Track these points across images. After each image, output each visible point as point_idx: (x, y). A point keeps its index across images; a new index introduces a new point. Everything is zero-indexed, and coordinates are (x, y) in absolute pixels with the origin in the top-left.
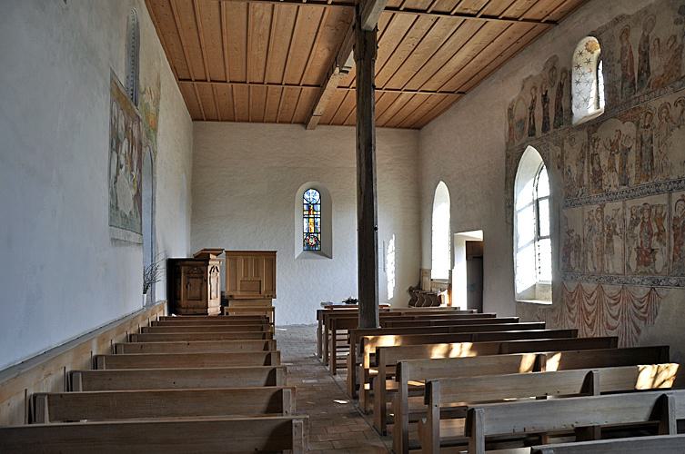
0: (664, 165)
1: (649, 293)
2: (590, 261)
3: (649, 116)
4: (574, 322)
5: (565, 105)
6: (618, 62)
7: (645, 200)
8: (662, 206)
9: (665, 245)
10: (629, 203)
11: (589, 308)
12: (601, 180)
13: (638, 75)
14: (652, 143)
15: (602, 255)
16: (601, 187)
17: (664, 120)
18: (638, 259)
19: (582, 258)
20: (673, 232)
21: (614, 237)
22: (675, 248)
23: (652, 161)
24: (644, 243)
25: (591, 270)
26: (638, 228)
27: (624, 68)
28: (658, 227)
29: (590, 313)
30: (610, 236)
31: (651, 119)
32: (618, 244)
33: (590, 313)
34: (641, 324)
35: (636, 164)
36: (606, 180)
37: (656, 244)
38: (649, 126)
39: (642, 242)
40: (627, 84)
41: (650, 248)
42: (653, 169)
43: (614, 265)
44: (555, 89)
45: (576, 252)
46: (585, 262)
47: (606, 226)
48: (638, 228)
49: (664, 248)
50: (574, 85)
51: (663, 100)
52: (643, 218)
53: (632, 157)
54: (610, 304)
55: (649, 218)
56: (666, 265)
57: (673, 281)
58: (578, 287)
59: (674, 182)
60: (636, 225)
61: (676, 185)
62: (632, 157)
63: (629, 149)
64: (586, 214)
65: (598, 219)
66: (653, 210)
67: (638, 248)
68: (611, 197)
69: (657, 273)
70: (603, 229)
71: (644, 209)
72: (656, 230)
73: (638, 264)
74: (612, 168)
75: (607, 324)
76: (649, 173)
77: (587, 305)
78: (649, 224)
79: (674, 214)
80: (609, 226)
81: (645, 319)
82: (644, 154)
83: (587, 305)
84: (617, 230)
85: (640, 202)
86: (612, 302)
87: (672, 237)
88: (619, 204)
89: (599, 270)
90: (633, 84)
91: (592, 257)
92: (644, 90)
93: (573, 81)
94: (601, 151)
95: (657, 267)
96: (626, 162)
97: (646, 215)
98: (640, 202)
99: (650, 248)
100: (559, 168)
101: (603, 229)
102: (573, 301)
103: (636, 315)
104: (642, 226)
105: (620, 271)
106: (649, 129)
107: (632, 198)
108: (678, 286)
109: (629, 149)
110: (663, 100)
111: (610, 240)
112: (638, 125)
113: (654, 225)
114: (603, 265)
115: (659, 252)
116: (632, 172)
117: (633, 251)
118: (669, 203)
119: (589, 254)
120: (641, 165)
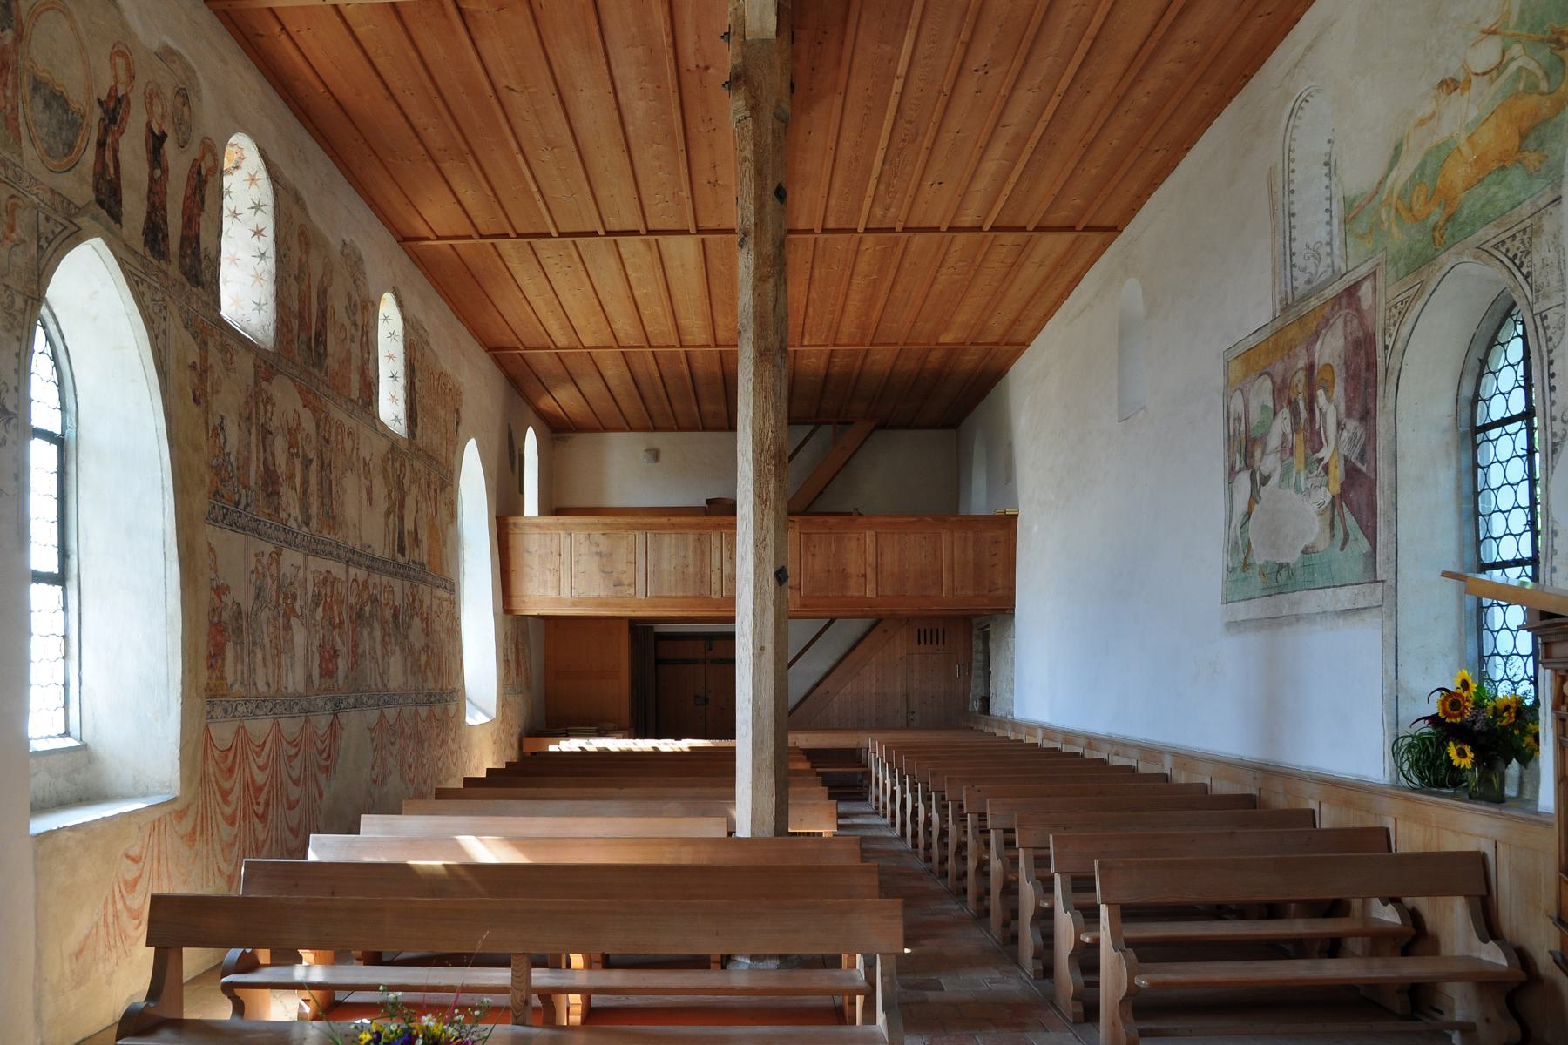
2: (260, 672)
4: (232, 824)
8: (342, 582)
11: (260, 778)
16: (277, 510)
18: (320, 665)
19: (246, 660)
21: (293, 621)
24: (326, 639)
25: (262, 687)
26: (320, 609)
29: (259, 790)
30: (287, 617)
32: (299, 636)
37: (339, 645)
39: (324, 635)
41: (333, 647)
43: (295, 680)
45: (235, 644)
46: (252, 670)
47: (282, 596)
48: (320, 609)
52: (326, 594)
54: (289, 757)
57: (352, 701)
58: (238, 731)
60: (318, 605)
64: (253, 559)
65: (272, 576)
67: (320, 646)
68: (290, 539)
70: (277, 602)
72: (337, 621)
73: (321, 675)
74: (291, 477)
77: (255, 770)
78: (331, 609)
80: (286, 598)
83: (255, 770)
86: (293, 751)
89: (273, 687)
91: (264, 660)
97: (329, 589)
101: (277, 602)
102: (231, 770)
105: (301, 689)
108: (355, 707)
111: (288, 627)
113: (335, 608)
114: (280, 675)
119: (259, 655)
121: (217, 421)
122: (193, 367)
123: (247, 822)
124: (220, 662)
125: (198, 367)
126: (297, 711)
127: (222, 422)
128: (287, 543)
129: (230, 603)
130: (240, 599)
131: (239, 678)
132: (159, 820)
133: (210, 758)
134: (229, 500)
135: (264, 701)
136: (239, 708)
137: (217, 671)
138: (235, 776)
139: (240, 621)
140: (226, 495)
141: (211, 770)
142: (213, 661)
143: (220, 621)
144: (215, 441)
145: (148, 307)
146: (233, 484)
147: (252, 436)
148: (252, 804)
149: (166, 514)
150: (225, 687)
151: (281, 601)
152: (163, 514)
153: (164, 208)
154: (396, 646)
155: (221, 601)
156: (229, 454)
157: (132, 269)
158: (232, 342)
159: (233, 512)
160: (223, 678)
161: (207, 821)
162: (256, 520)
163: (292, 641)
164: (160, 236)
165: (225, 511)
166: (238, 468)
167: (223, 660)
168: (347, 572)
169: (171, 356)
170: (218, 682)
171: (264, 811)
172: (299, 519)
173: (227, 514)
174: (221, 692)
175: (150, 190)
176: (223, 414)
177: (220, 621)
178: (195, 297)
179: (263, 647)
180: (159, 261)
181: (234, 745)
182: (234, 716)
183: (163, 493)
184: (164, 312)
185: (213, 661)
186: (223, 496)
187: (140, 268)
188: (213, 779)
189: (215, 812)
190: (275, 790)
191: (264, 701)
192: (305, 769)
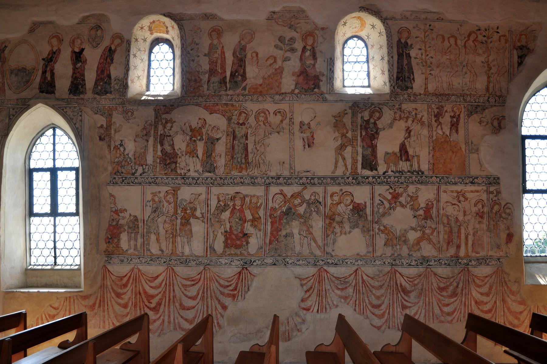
0: (261, 161)
1: (240, 273)
3: (243, 115)
5: (115, 72)
6: (205, 55)
7: (237, 189)
8: (258, 197)
9: (260, 230)
10: (215, 190)
12: (176, 163)
13: (231, 75)
14: (247, 139)
15: (174, 236)
17: (261, 123)
20: (270, 220)
21: (192, 220)
22: (272, 234)
23: (247, 155)
24: (234, 228)
27: (211, 62)
28: (252, 215)
29: (153, 297)
31: (247, 118)
33: (153, 297)
34: (227, 301)
35: (226, 155)
36: (183, 164)
38: (243, 124)
40: (216, 79)
41: (242, 232)
42: (247, 163)
44: (99, 51)
49: (259, 233)
50: (132, 57)
51: (261, 106)
53: (221, 148)
54: (185, 286)
55: (242, 206)
56: (261, 248)
57: (269, 261)
59: (272, 178)
60: (224, 210)
61: (274, 181)
62: (221, 148)
63: (218, 139)
66: (248, 200)
67: (226, 232)
69: (250, 254)
71: (235, 197)
75: (181, 305)
76: (244, 166)
78: (242, 211)
79: (270, 205)
80: (185, 210)
81: (234, 296)
82: (236, 147)
84: (198, 213)
85: (231, 190)
87: (269, 223)
88: (201, 189)
89: (167, 252)
90: (223, 81)
92: (238, 91)
93: (132, 53)
94: (177, 133)
95: (250, 250)
96: (213, 150)
97: (238, 202)
98: (231, 190)
99: (242, 232)
100: (101, 139)
102: (125, 286)
103: (222, 293)
104: (232, 212)
106: (244, 127)
107: (220, 185)
108: (275, 264)
109: (218, 139)
110: (261, 106)
112: (229, 120)
115: (254, 236)
116: (221, 162)
117: (219, 235)
118: (267, 195)
119: (153, 237)
120: (232, 157)
121: (118, 143)
122: (102, 126)
123: (138, 308)
124: (116, 240)
125: (105, 126)
126: (194, 264)
127: (122, 143)
128: (184, 184)
129: (128, 216)
130: (138, 214)
131: (133, 247)
132: (70, 297)
133: (108, 278)
134: (129, 173)
135: (158, 258)
136: (134, 260)
137: (113, 244)
138: (128, 288)
139: (136, 223)
140: (124, 172)
141: (109, 283)
142: (111, 241)
143: (117, 224)
144: (116, 152)
146: (132, 166)
147: (150, 142)
148: (143, 302)
150: (121, 251)
151: (179, 212)
153: (83, 75)
154: (353, 228)
155: (119, 216)
156: (128, 155)
158: (132, 107)
159: (130, 178)
160: (118, 246)
161: (104, 304)
162: (154, 178)
163: (191, 230)
164: (80, 87)
165: (124, 178)
166: (135, 159)
167: (119, 240)
168: (267, 190)
170: (114, 249)
171: (156, 306)
172: (201, 170)
173: (126, 179)
174: (117, 253)
175: (74, 73)
176: (122, 139)
177: (117, 224)
178: (103, 100)
179: (157, 234)
181: (129, 275)
182: (129, 263)
184: (80, 114)
185: (111, 241)
186: (122, 173)
188: (110, 287)
189: (111, 301)
190: (167, 299)
191: (158, 258)
192: (203, 292)
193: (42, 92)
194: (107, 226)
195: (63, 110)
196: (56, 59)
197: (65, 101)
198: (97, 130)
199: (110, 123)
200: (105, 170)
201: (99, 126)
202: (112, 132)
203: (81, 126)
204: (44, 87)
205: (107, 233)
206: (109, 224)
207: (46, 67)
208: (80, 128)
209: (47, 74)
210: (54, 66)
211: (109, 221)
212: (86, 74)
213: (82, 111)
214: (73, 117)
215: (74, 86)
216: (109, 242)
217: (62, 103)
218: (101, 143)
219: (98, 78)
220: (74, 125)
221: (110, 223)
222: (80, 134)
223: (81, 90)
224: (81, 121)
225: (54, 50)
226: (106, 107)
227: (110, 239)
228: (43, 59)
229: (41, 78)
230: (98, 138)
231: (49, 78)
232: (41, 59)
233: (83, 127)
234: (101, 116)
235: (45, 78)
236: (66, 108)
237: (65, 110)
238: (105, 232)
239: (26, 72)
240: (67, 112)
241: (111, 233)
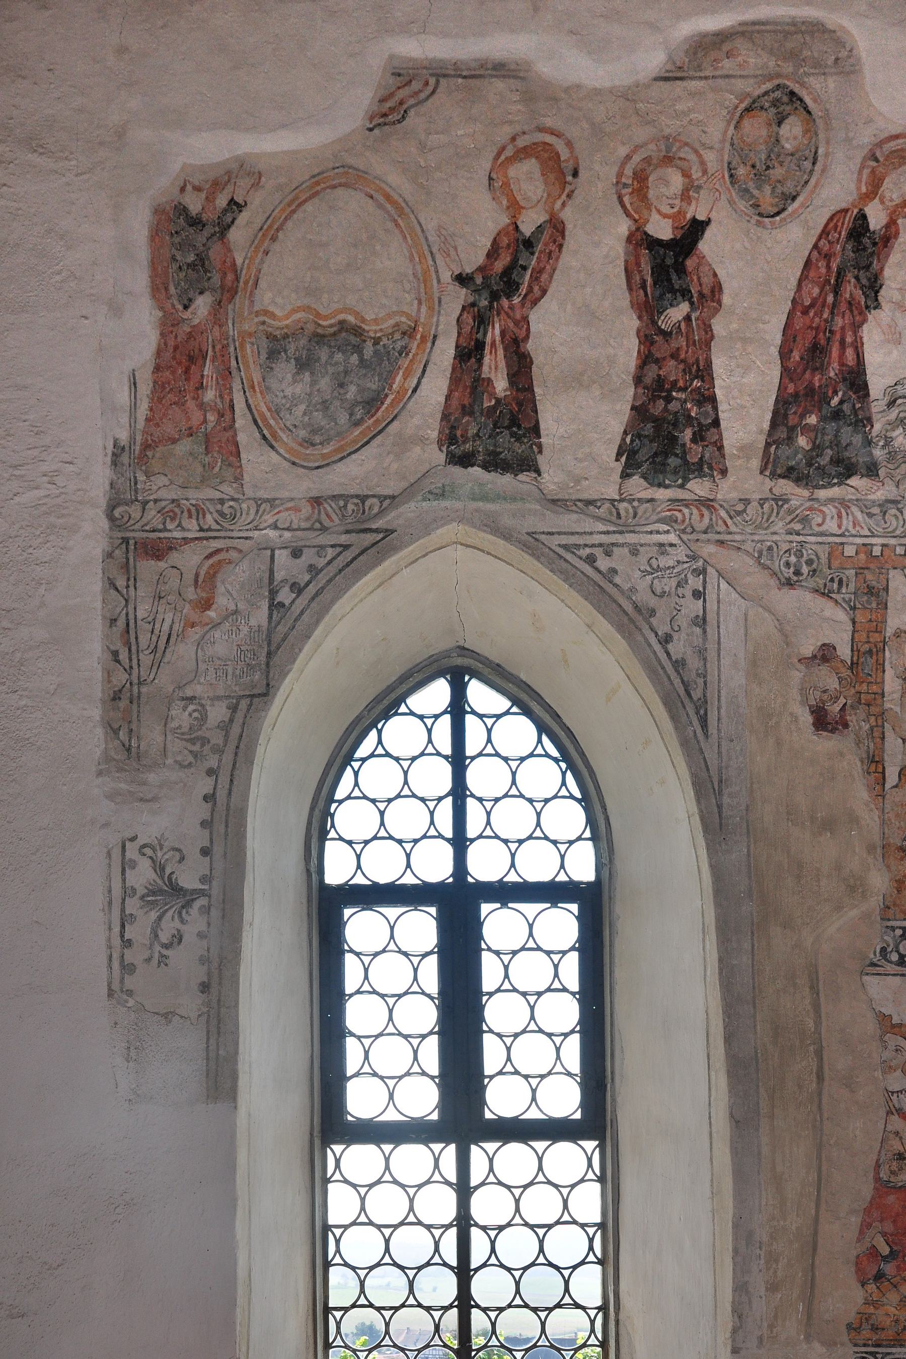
122: (826, 654)
142: (889, 1269)
145: (633, 590)
149: (708, 979)
152: (705, 979)
153: (705, 372)
157: (564, 540)
169: (726, 661)
175: (646, 359)
180: (682, 486)
183: (704, 940)
184: (695, 582)
187: (601, 527)
193: (464, 460)
194: (867, 1190)
195: (591, 560)
196: (535, 278)
197: (602, 512)
198: (797, 675)
199: (875, 637)
200: (852, 889)
201: (808, 650)
202: (887, 689)
203: (701, 653)
204: (472, 431)
205: (865, 1226)
206: (877, 1179)
207: (482, 321)
208: (694, 663)
209: (487, 360)
210: (526, 319)
211: (878, 1166)
212: (719, 364)
213: (704, 572)
214: (653, 602)
215: (649, 429)
216: (879, 1276)
217: (588, 525)
218: (827, 743)
219: (791, 388)
220: (657, 647)
221: (884, 1175)
222: (697, 694)
223: (695, 452)
224: (701, 621)
225: (527, 229)
226: (850, 551)
227: (885, 1259)
228: (462, 279)
229: (455, 381)
230: (807, 719)
231: (501, 385)
232: (446, 276)
233: (711, 655)
234: (821, 601)
235: (480, 385)
236: (608, 554)
237: (603, 563)
238: (855, 1221)
239: (358, 349)
240: (614, 571)
241: (889, 1227)
